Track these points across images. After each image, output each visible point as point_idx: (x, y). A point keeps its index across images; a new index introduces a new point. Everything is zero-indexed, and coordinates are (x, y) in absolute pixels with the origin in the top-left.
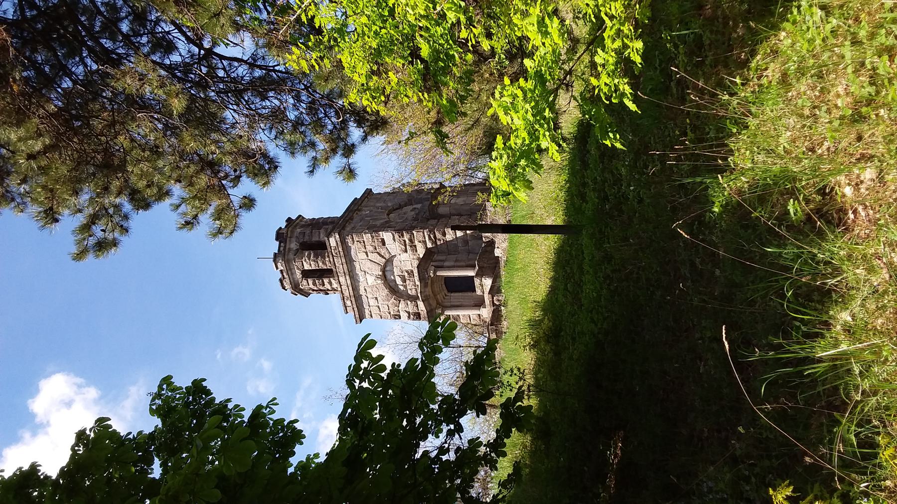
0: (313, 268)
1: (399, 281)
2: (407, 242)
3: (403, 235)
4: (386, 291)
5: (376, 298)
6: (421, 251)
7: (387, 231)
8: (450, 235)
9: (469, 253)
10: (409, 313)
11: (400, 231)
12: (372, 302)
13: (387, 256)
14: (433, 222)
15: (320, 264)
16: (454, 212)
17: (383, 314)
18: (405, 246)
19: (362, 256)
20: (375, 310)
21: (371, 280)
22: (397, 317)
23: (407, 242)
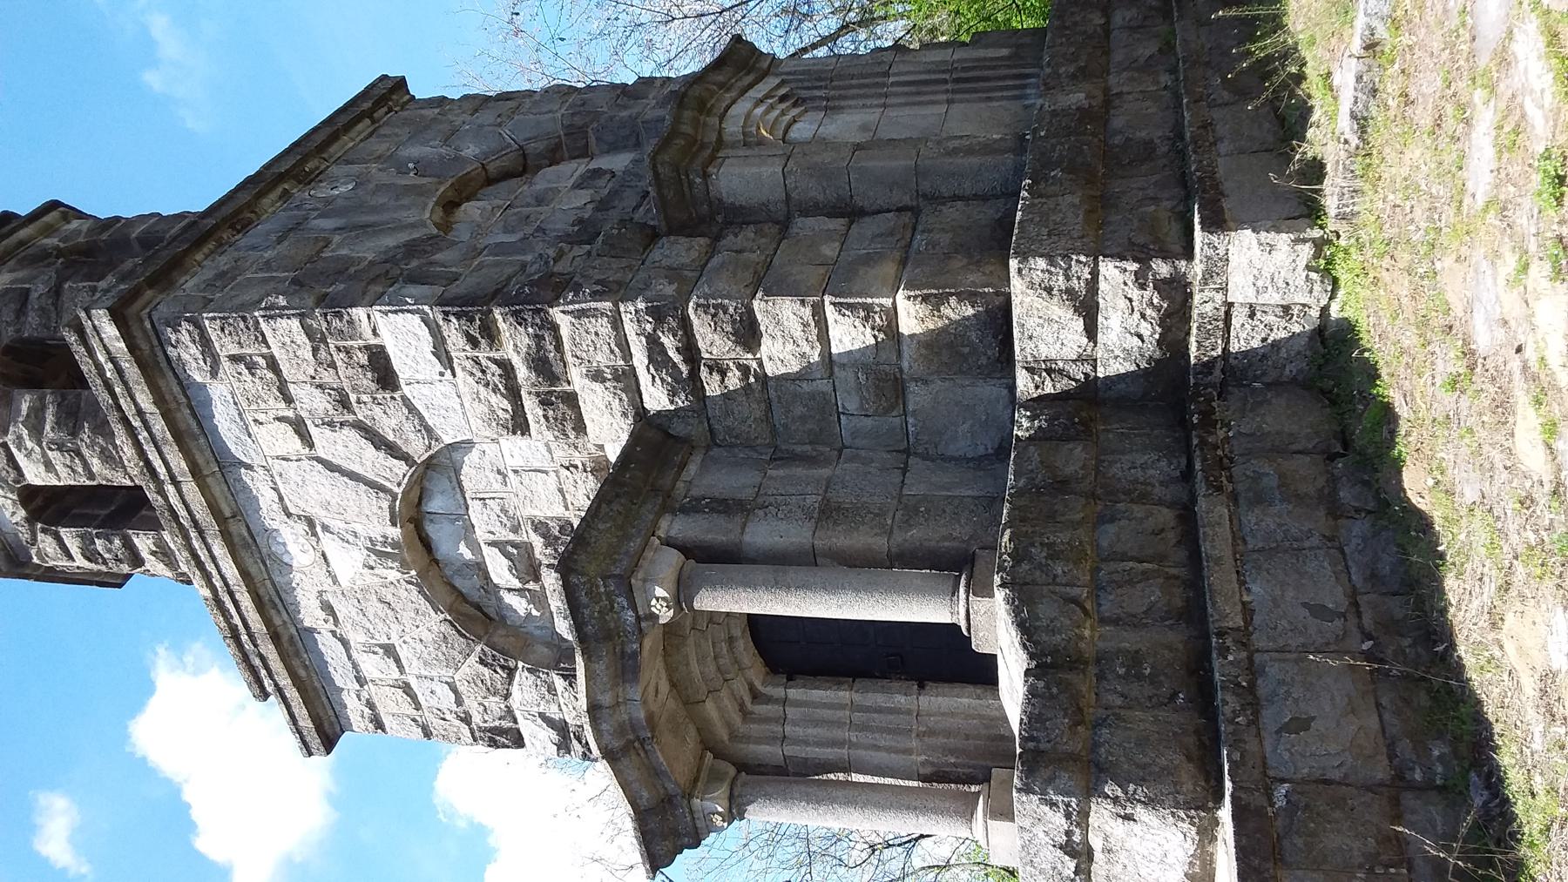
0: (65, 479)
1: (500, 570)
2: (522, 372)
4: (433, 623)
5: (390, 651)
6: (609, 431)
8: (786, 338)
9: (905, 452)
10: (561, 728)
11: (472, 305)
12: (372, 666)
13: (418, 448)
14: (680, 251)
15: (96, 464)
16: (812, 189)
18: (513, 394)
19: (278, 440)
20: (391, 704)
21: (349, 563)
22: (506, 736)
23: (522, 372)
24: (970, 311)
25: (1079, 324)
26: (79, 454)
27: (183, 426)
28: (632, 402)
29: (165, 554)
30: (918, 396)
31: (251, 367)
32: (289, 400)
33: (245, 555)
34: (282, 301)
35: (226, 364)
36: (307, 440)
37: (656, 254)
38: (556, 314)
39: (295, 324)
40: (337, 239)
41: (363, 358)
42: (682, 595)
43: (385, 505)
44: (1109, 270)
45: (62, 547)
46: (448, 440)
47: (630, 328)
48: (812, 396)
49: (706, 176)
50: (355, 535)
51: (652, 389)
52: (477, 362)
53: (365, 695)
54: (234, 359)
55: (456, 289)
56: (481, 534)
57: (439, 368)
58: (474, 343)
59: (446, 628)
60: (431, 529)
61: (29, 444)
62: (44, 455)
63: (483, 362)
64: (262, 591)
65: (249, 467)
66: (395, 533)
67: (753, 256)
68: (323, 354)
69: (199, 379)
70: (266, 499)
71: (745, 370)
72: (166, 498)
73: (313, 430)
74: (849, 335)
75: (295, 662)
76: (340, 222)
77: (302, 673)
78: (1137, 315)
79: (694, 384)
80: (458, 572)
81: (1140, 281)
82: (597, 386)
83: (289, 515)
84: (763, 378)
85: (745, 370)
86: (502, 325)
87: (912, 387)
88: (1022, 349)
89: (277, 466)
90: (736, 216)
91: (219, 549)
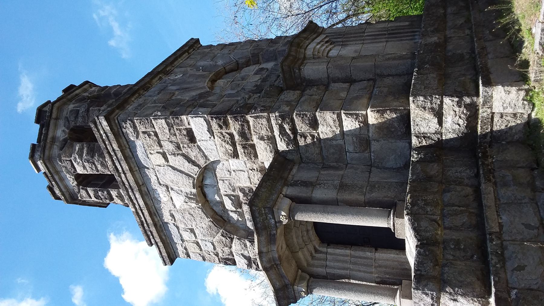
1: (228, 204)
2: (237, 137)
3: (226, 124)
5: (192, 231)
6: (266, 157)
7: (196, 115)
8: (327, 126)
9: (370, 166)
10: (248, 259)
11: (219, 115)
12: (187, 236)
13: (202, 162)
14: (290, 95)
15: (99, 167)
16: (337, 73)
17: (207, 256)
18: (234, 144)
20: (192, 249)
21: (179, 201)
22: (230, 261)
24: (395, 116)
25: (436, 120)
26: (94, 164)
27: (127, 155)
28: (274, 147)
29: (120, 197)
30: (375, 146)
31: (149, 135)
32: (161, 146)
33: (146, 197)
34: (159, 114)
35: (141, 134)
36: (166, 160)
37: (282, 97)
38: (249, 118)
39: (163, 121)
40: (177, 93)
41: (185, 132)
42: (291, 215)
43: (191, 181)
44: (447, 101)
45: (89, 194)
46: (212, 160)
47: (273, 122)
48: (337, 146)
49: (300, 69)
50: (181, 191)
51: (281, 143)
52: (222, 134)
53: (184, 245)
54: (144, 133)
55: (216, 109)
56: (222, 192)
57: (209, 136)
58: (221, 127)
59: (210, 223)
60: (206, 190)
61: (78, 160)
62: (83, 164)
63: (224, 134)
64: (151, 210)
65: (148, 168)
66: (194, 191)
67: (316, 97)
68: (172, 131)
69: (132, 139)
70: (153, 179)
71: (313, 136)
72: (121, 178)
73: (168, 156)
74: (350, 124)
75: (162, 234)
76: (178, 87)
77: (164, 237)
78: (457, 117)
79: (295, 141)
80: (215, 205)
81: (459, 104)
82: (262, 142)
83: (160, 184)
84: (319, 139)
85: (313, 136)
86: (230, 121)
87: (373, 142)
88: (414, 129)
89: (157, 168)
90: (310, 83)
91: (138, 195)
